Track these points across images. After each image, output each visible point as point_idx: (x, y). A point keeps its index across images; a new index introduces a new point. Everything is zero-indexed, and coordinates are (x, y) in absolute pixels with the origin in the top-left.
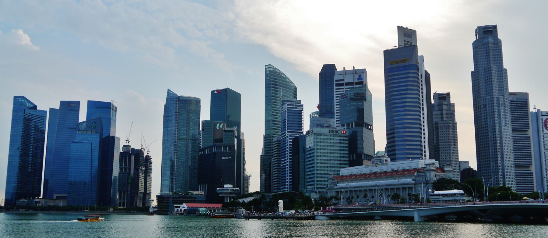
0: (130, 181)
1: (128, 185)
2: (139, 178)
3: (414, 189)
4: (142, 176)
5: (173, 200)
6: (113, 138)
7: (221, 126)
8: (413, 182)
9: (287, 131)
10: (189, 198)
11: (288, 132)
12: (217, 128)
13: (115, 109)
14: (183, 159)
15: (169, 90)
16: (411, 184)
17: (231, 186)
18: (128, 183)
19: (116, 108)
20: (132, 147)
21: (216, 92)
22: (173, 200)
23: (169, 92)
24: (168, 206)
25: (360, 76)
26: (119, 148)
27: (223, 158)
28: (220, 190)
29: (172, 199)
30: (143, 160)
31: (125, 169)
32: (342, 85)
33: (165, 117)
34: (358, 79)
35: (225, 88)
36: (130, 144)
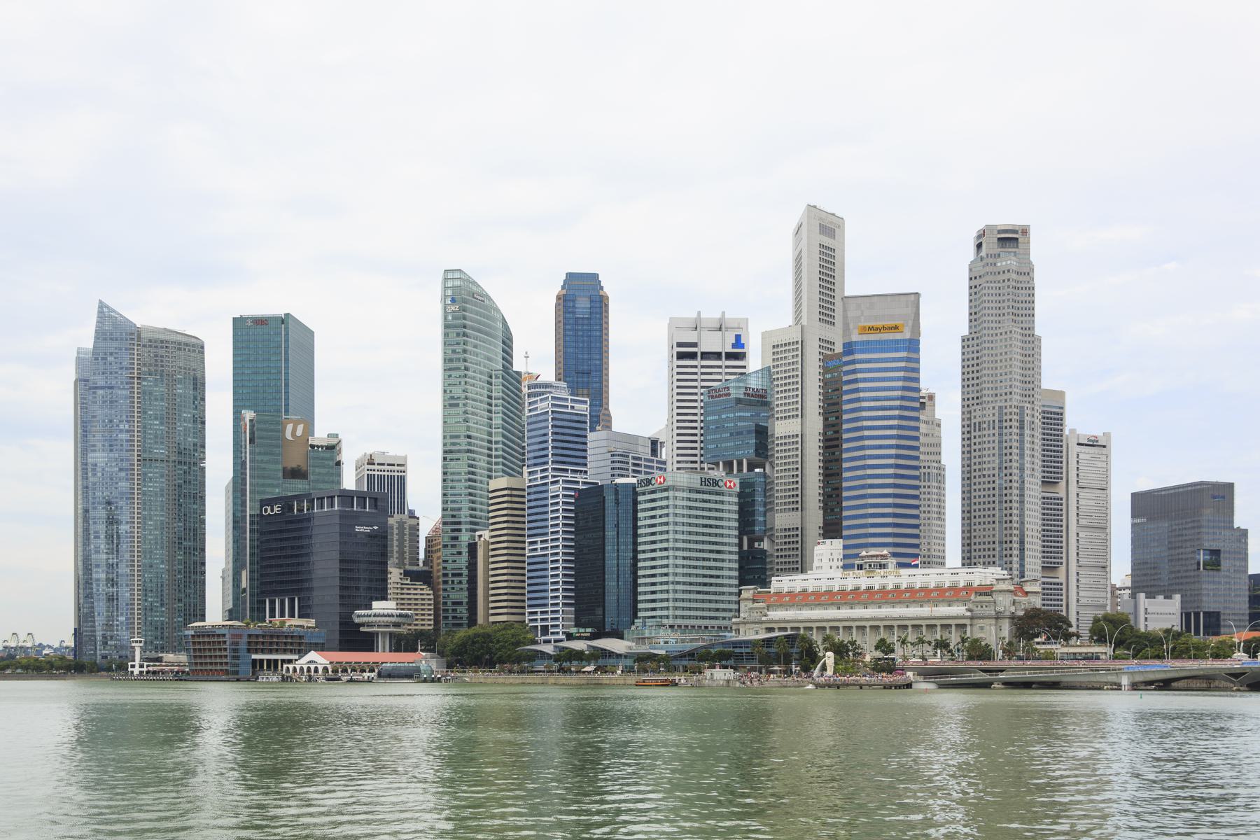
3: (969, 628)
7: (299, 432)
8: (969, 614)
9: (550, 466)
11: (554, 469)
12: (288, 436)
15: (102, 305)
16: (964, 617)
23: (104, 313)
25: (738, 337)
27: (358, 529)
29: (245, 639)
32: (692, 356)
34: (734, 346)
35: (280, 311)
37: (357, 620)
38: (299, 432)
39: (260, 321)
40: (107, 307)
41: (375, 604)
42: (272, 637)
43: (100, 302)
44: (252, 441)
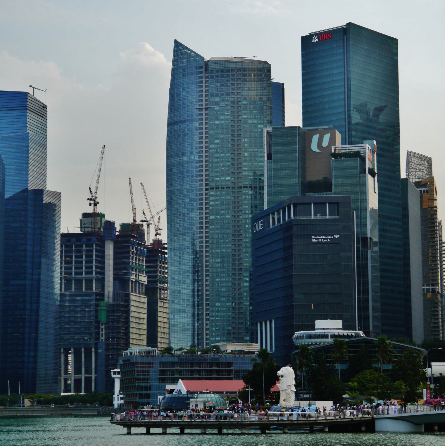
0: (103, 317)
1: (98, 328)
2: (127, 306)
4: (138, 303)
5: (163, 372)
6: (39, 193)
7: (325, 143)
10: (211, 364)
12: (314, 147)
13: (42, 110)
14: (227, 247)
15: (177, 44)
17: (338, 324)
18: (98, 322)
19: (45, 107)
20: (108, 218)
21: (315, 40)
22: (163, 372)
24: (149, 388)
26: (69, 222)
27: (315, 239)
28: (301, 337)
29: (157, 368)
30: (139, 253)
31: (89, 282)
33: (172, 123)
36: (100, 209)
37: (299, 342)
38: (325, 143)
39: (326, 36)
40: (181, 45)
41: (320, 324)
42: (192, 364)
43: (176, 41)
44: (269, 157)
